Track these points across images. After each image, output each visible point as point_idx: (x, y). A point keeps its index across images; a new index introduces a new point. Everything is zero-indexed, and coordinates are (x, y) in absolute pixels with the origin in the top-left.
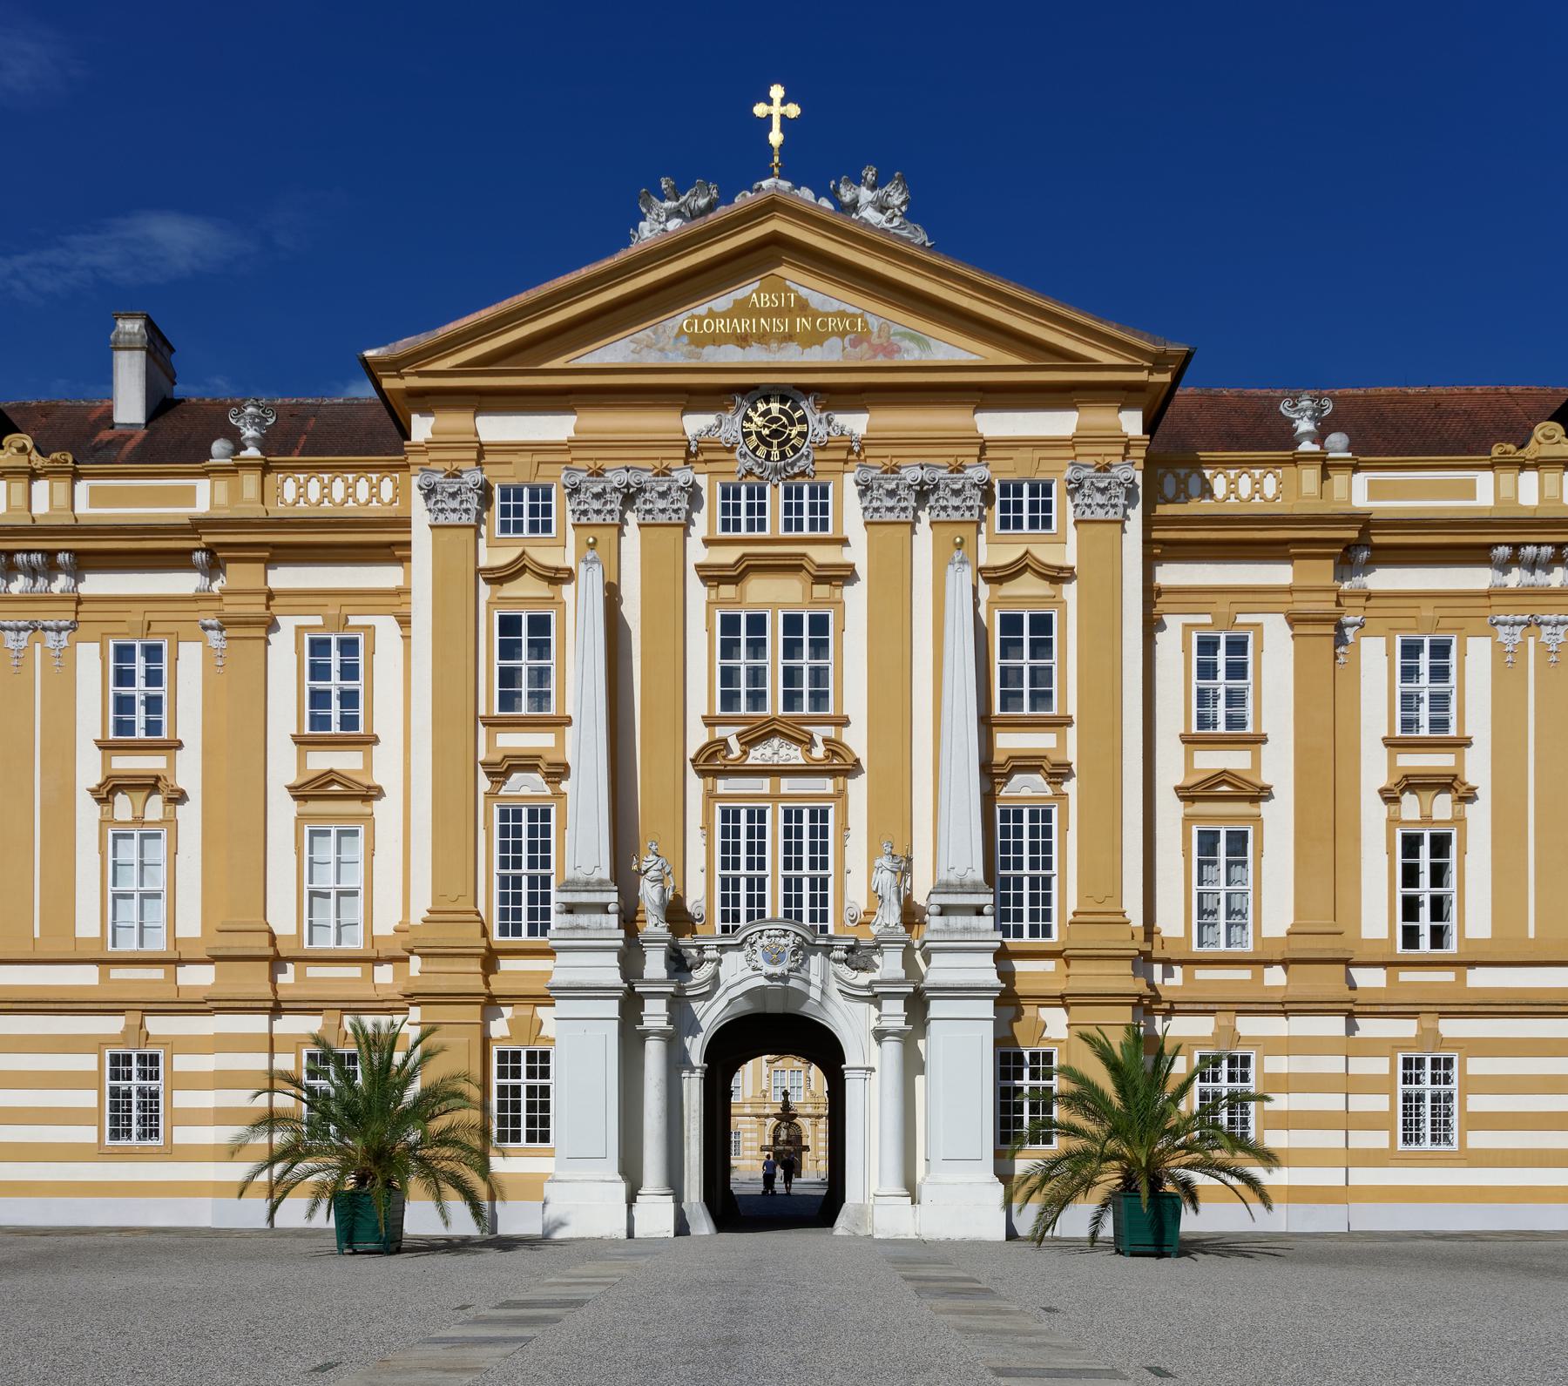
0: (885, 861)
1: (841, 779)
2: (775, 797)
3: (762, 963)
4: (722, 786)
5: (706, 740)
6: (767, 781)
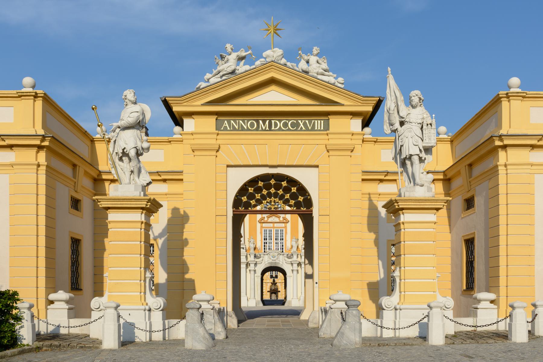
0: (294, 240)
1: (286, 224)
2: (274, 227)
3: (271, 258)
4: (264, 225)
5: (261, 217)
6: (272, 224)
